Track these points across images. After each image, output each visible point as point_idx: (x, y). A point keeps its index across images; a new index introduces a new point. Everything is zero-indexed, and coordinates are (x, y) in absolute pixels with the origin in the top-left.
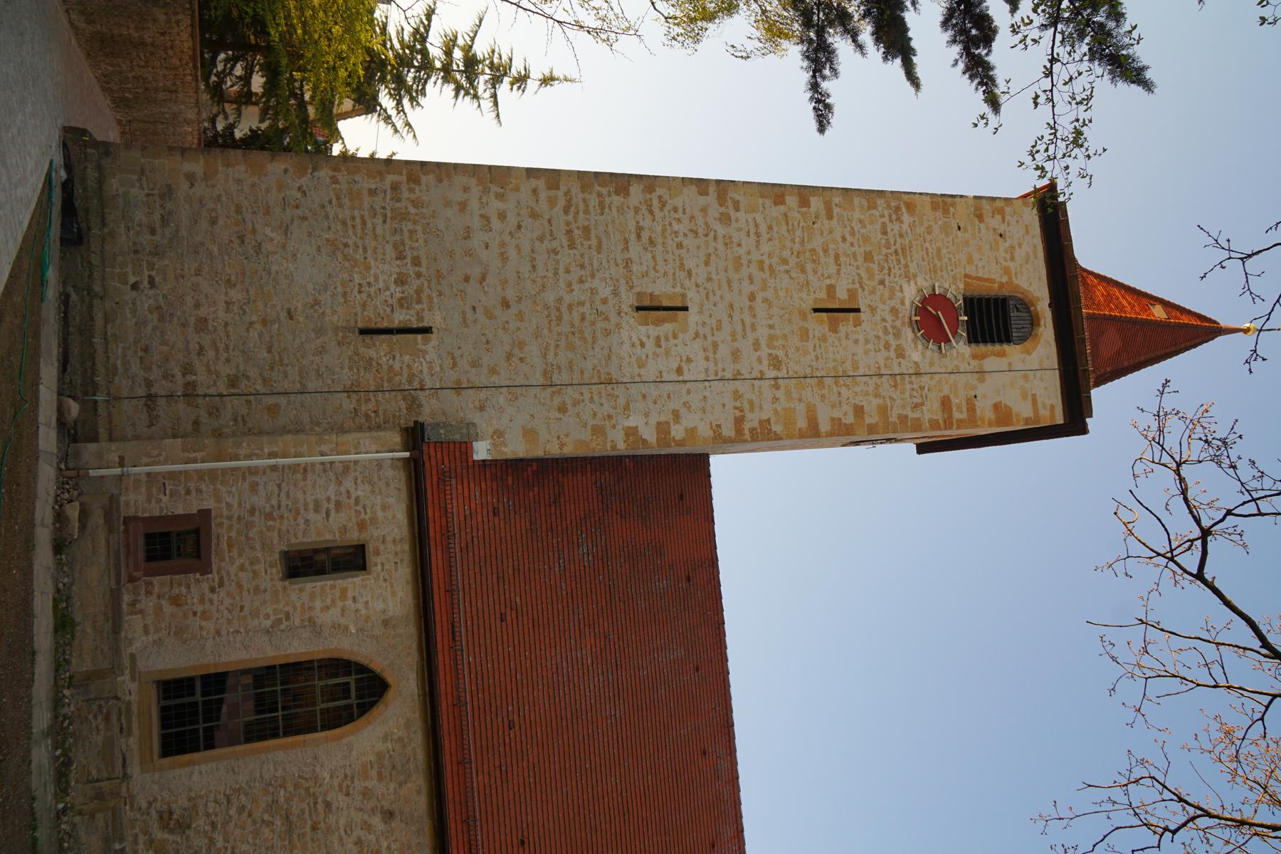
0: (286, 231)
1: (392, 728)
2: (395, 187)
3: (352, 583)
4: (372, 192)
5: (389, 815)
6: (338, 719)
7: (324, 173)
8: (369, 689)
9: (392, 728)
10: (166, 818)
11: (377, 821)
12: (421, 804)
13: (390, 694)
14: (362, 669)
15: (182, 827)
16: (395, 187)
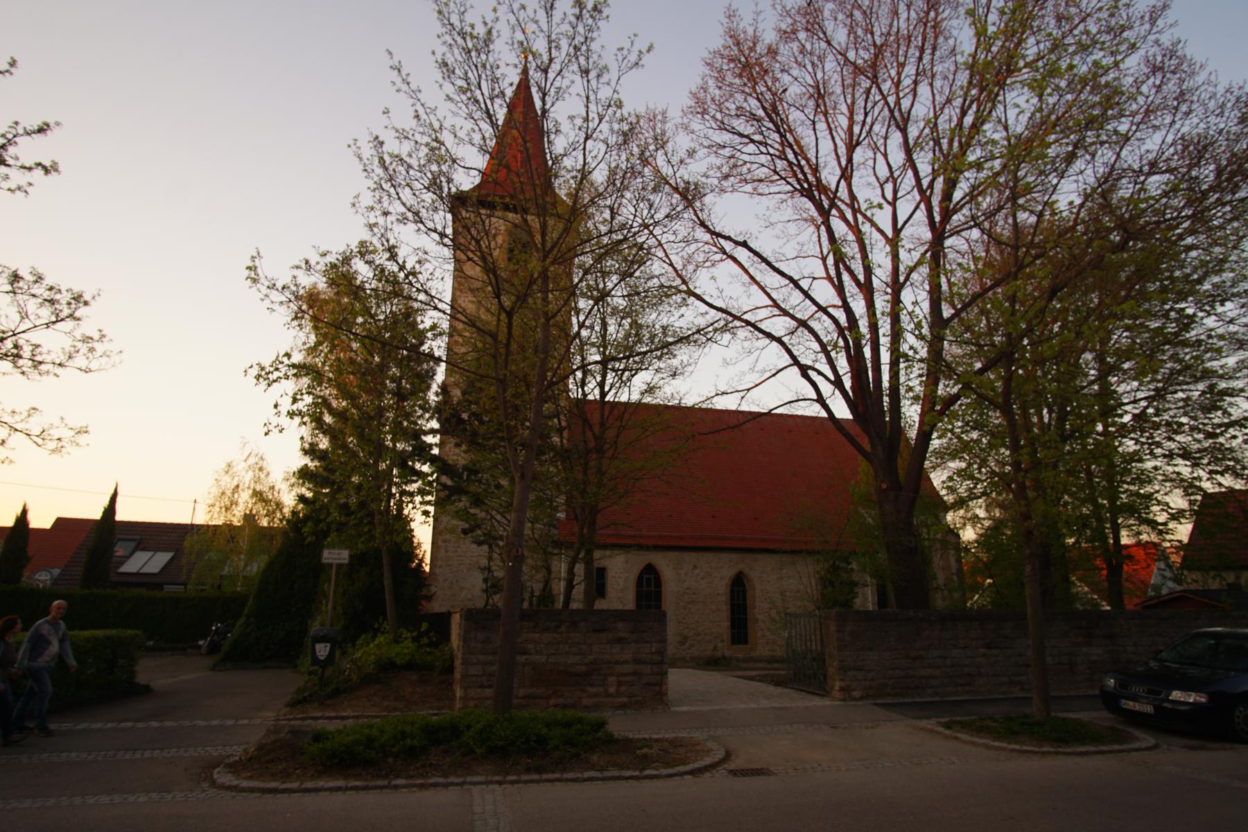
0: (462, 588)
1: (665, 564)
2: (444, 541)
3: (610, 575)
4: (446, 551)
5: (695, 567)
6: (658, 582)
7: (437, 571)
8: (650, 569)
9: (665, 564)
10: (682, 643)
11: (696, 571)
12: (693, 555)
13: (653, 562)
14: (641, 573)
15: (686, 638)
16: (444, 541)
